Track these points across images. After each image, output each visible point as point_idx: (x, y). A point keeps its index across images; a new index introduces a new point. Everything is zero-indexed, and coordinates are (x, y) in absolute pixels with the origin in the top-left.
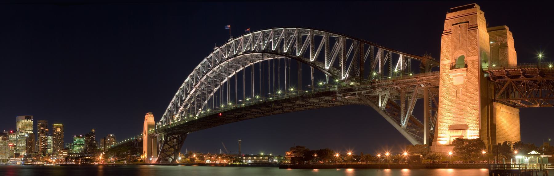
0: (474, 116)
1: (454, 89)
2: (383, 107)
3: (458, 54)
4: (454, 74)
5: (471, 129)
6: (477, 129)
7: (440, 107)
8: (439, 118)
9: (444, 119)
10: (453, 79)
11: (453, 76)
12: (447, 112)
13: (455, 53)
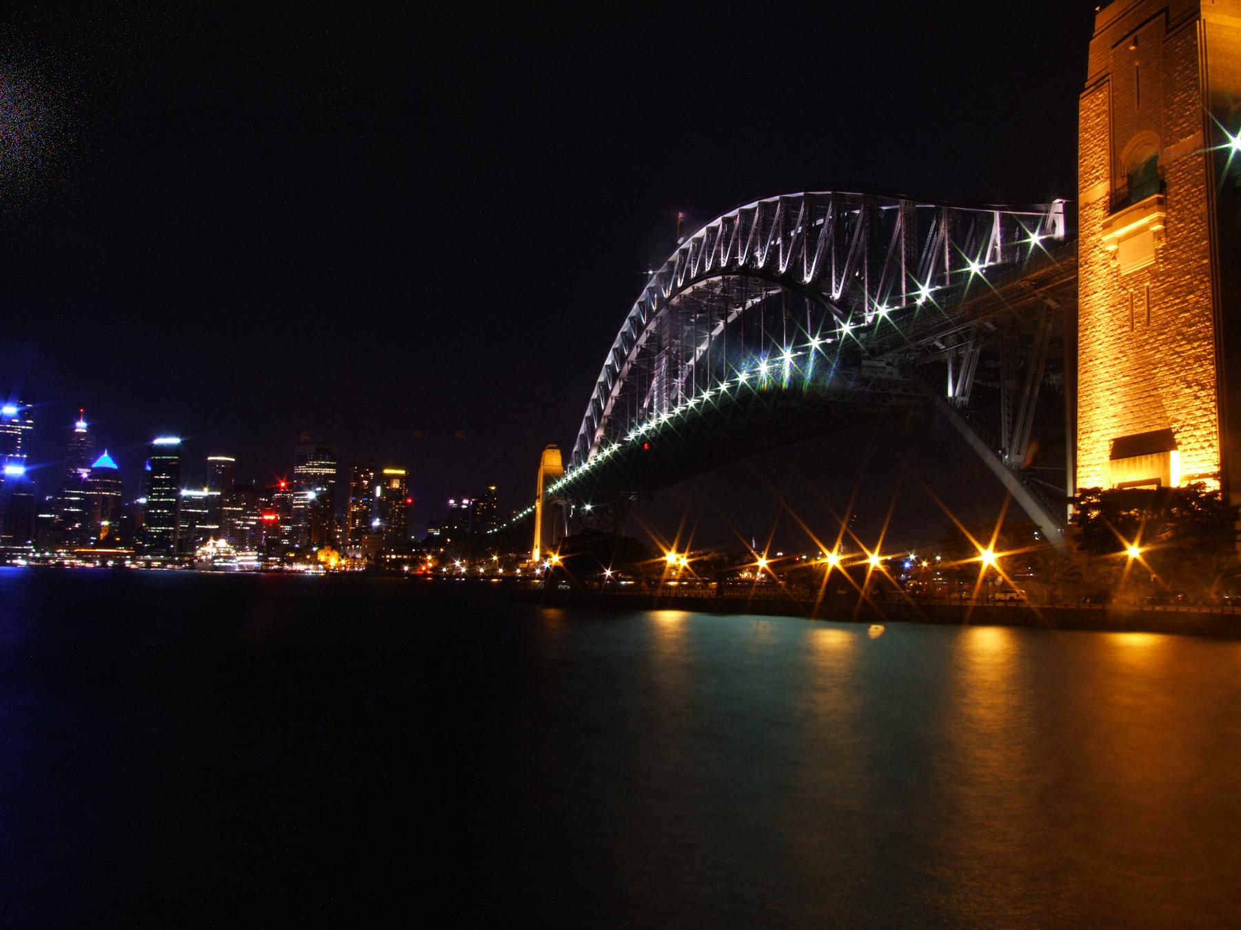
0: (1196, 388)
1: (1125, 292)
2: (960, 399)
3: (1142, 148)
4: (1120, 232)
5: (1189, 447)
6: (1211, 446)
7: (1083, 371)
8: (1079, 414)
10: (1117, 251)
11: (1119, 241)
13: (1124, 152)
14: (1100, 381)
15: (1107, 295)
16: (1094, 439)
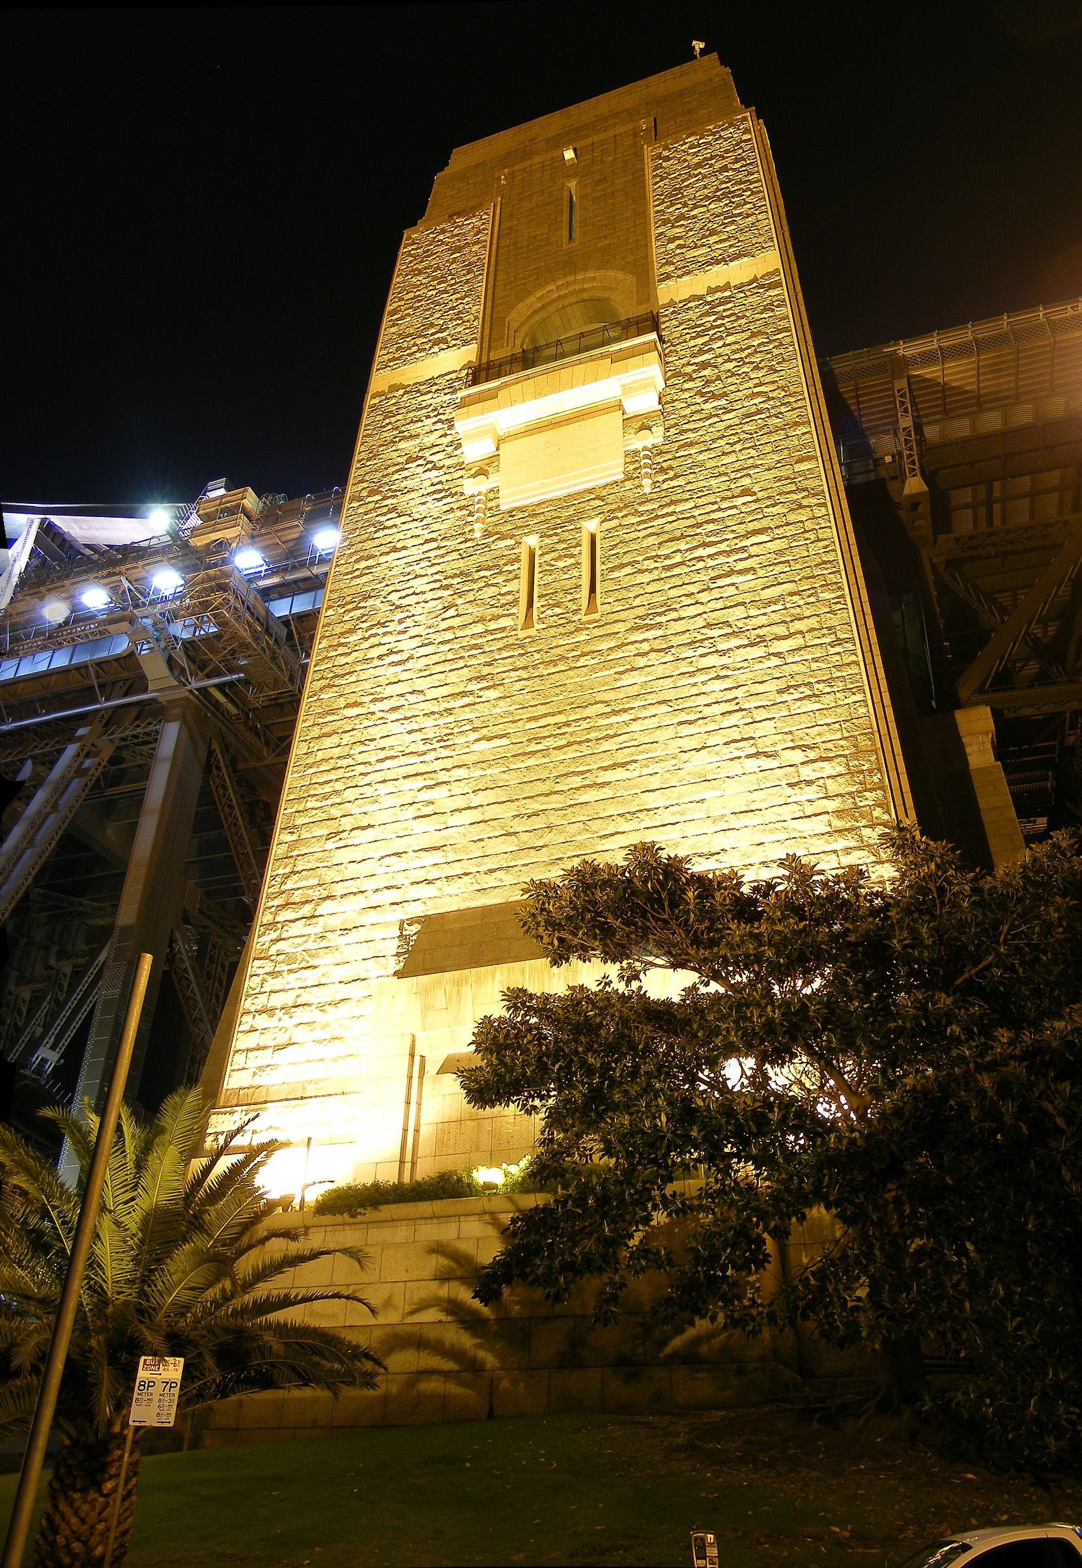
0: (797, 756)
9: (343, 856)
12: (394, 768)
14: (382, 755)
15: (443, 551)
16: (335, 922)
